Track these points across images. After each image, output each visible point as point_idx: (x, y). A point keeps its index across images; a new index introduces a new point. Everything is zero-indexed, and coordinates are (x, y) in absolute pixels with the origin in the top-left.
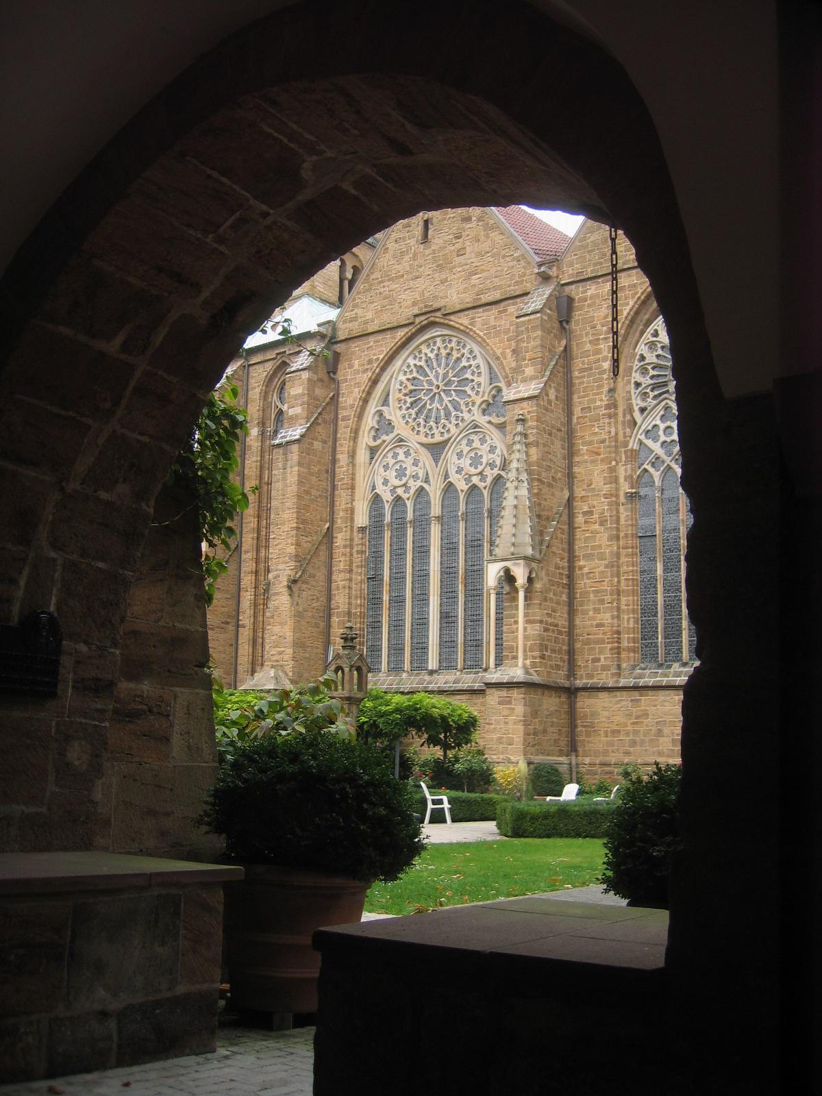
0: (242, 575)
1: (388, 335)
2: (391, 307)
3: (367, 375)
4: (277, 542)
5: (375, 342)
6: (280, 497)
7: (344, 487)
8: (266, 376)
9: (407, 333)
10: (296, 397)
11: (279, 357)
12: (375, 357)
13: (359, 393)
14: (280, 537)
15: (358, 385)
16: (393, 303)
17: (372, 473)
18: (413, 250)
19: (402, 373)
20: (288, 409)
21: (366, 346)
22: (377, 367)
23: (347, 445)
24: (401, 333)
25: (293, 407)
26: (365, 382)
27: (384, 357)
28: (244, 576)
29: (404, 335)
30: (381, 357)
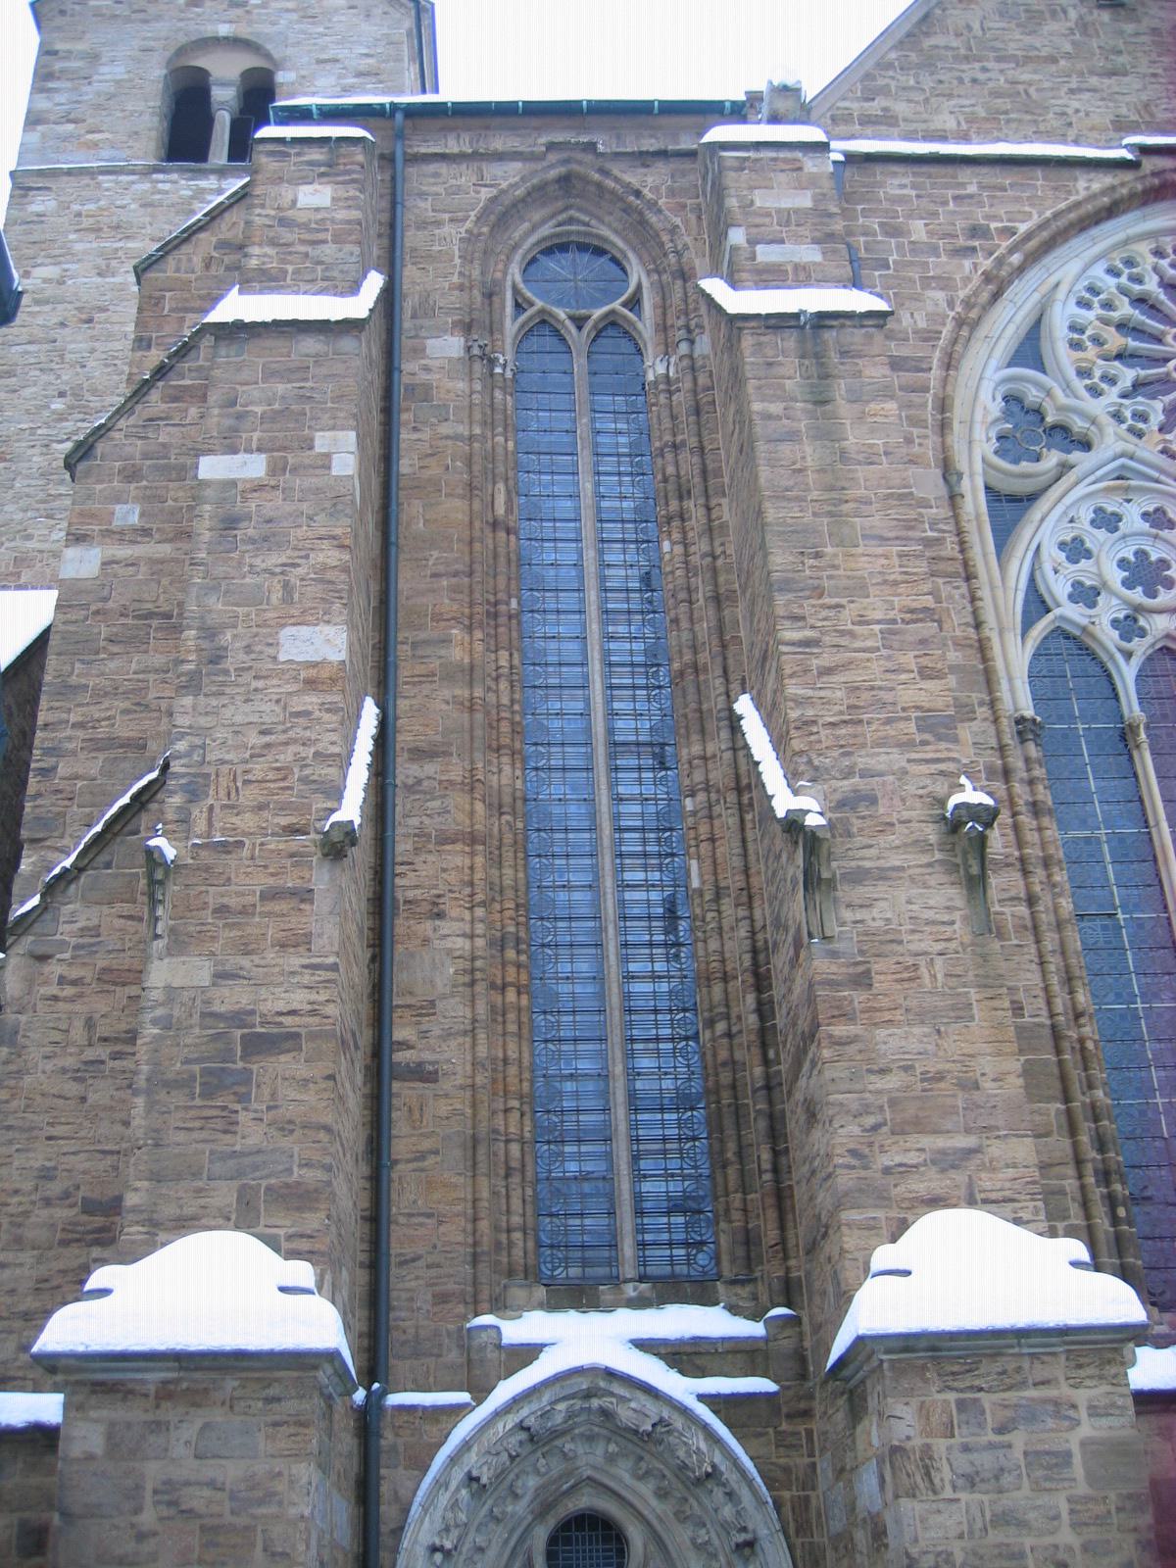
0: (402, 847)
1: (1039, 178)
2: (1029, 117)
3: (975, 265)
4: (827, 659)
5: (981, 187)
6: (814, 495)
7: (942, 566)
8: (493, 200)
9: (1113, 188)
10: (787, 217)
11: (552, 157)
12: (993, 225)
13: (951, 304)
14: (843, 641)
15: (945, 283)
16: (1038, 111)
17: (1030, 554)
18: (1073, 14)
19: (1072, 301)
20: (753, 242)
21: (950, 193)
22: (1011, 251)
23: (929, 443)
24: (1087, 185)
25: (782, 242)
26: (967, 280)
27: (1028, 236)
28: (417, 850)
29: (1103, 193)
30: (1023, 228)
